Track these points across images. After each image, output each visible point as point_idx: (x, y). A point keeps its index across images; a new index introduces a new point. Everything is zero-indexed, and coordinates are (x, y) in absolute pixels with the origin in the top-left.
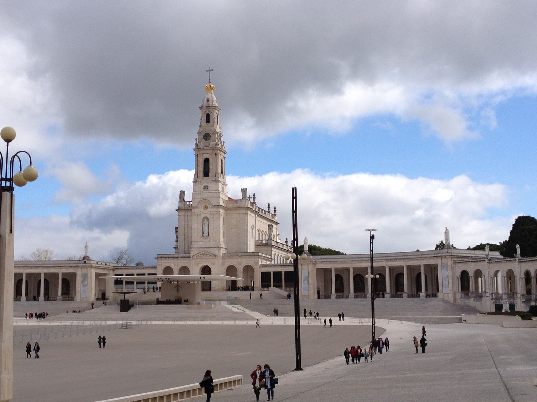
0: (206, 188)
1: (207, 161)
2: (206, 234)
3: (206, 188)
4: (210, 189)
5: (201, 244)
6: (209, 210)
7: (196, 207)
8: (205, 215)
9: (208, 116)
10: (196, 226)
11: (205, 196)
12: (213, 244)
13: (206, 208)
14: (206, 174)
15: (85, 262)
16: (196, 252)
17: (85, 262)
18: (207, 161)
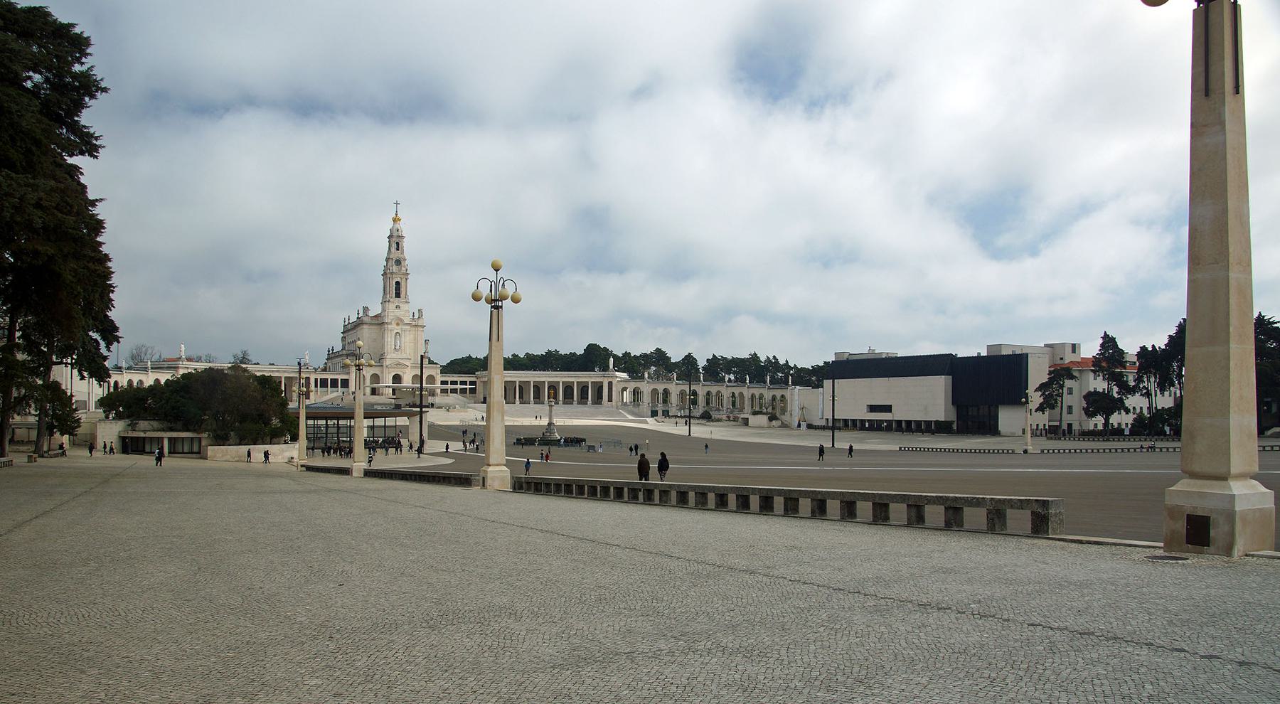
0: (398, 307)
1: (398, 283)
2: (397, 347)
3: (398, 307)
4: (402, 308)
5: (394, 356)
6: (400, 327)
7: (391, 324)
8: (398, 331)
9: (398, 243)
10: (389, 340)
11: (398, 314)
12: (404, 356)
13: (398, 324)
14: (398, 295)
15: (307, 368)
16: (390, 362)
17: (307, 368)
18: (398, 283)
